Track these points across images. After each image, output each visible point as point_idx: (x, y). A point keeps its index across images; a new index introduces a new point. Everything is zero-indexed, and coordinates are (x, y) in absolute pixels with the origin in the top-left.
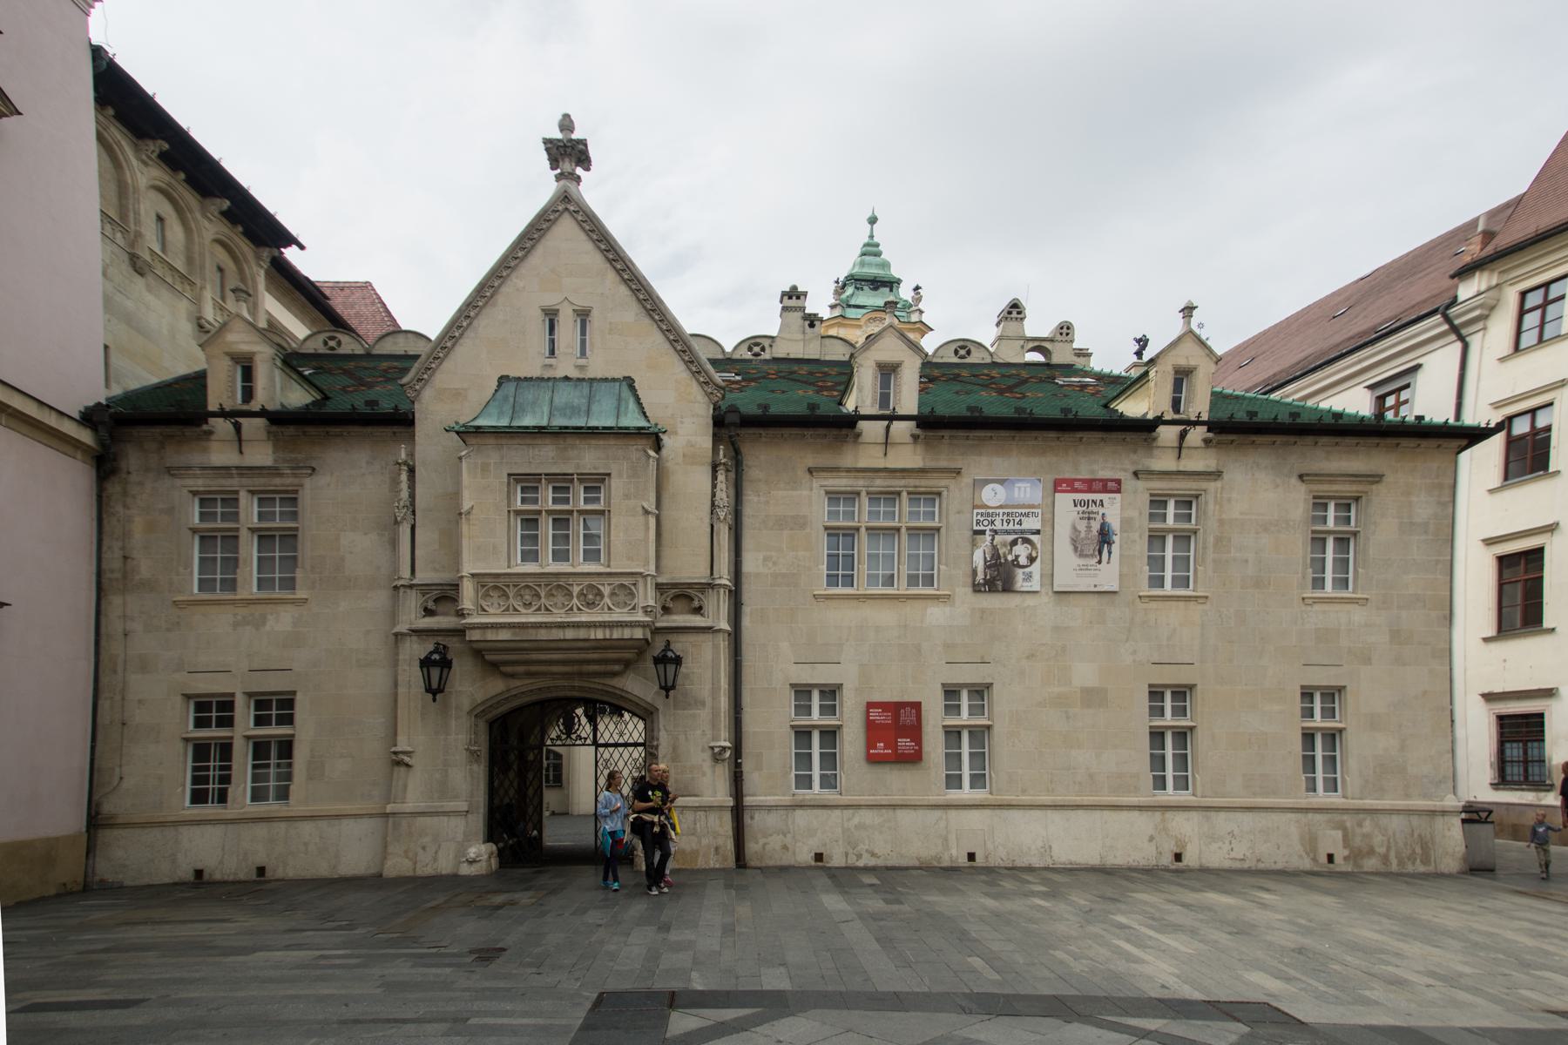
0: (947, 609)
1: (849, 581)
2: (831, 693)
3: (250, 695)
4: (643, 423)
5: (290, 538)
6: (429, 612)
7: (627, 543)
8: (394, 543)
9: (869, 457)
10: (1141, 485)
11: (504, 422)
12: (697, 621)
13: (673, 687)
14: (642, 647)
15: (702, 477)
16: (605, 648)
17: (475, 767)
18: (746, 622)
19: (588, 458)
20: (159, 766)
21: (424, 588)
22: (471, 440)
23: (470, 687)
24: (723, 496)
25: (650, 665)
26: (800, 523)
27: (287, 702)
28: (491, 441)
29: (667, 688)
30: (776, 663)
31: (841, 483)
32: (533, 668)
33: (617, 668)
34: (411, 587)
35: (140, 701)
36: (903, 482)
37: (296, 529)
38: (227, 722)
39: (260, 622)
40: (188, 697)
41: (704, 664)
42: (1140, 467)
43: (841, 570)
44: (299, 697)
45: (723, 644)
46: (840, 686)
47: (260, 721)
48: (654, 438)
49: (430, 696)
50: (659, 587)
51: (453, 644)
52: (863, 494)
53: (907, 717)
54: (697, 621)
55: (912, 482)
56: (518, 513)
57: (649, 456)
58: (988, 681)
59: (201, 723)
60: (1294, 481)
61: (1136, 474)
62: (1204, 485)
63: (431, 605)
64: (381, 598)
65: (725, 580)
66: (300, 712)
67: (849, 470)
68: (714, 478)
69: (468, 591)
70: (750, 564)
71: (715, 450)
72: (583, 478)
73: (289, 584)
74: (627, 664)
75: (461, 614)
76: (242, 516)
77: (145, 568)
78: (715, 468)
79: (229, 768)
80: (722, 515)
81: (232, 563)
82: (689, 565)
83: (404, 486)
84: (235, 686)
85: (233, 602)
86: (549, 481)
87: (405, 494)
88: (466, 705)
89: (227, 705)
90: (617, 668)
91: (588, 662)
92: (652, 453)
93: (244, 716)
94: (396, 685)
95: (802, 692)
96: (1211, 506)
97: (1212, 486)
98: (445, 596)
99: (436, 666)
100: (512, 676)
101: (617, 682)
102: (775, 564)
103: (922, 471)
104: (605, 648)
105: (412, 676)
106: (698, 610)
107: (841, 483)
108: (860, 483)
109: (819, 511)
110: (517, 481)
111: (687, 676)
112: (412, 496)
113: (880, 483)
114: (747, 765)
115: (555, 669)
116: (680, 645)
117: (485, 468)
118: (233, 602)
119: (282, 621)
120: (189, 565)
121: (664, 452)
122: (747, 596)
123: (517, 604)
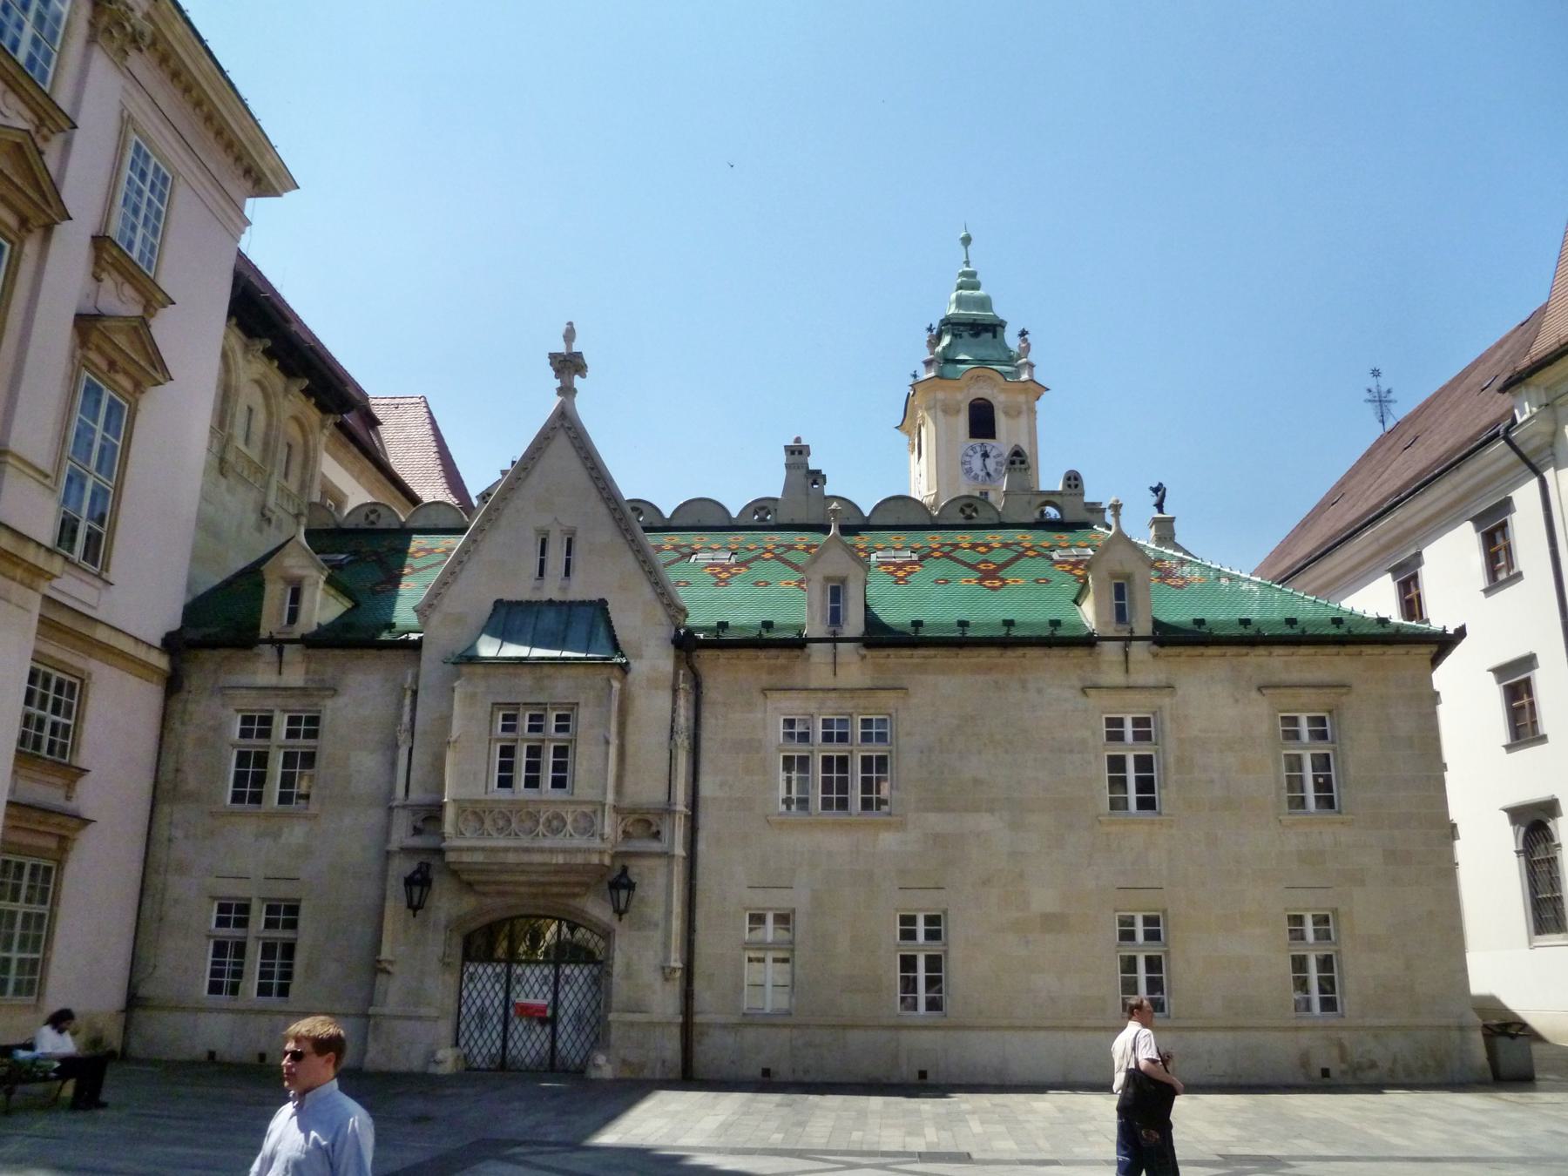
3: (264, 900)
6: (417, 831)
7: (592, 767)
8: (393, 765)
12: (655, 846)
15: (663, 700)
18: (702, 846)
20: (187, 961)
22: (465, 669)
24: (684, 719)
25: (606, 886)
27: (293, 909)
33: (577, 890)
35: (176, 901)
38: (242, 923)
39: (276, 836)
40: (214, 898)
41: (659, 887)
42: (1088, 684)
44: (303, 904)
45: (679, 870)
46: (794, 911)
47: (269, 924)
49: (411, 912)
51: (435, 862)
59: (222, 922)
60: (1254, 694)
61: (1084, 690)
63: (419, 824)
64: (375, 816)
65: (681, 805)
68: (675, 702)
69: (450, 814)
70: (707, 787)
71: (676, 674)
72: (555, 706)
77: (191, 781)
78: (675, 691)
80: (679, 741)
81: (260, 780)
82: (647, 788)
83: (407, 709)
84: (253, 892)
87: (406, 718)
89: (244, 908)
90: (577, 890)
91: (551, 884)
93: (258, 917)
96: (1168, 726)
97: (1166, 701)
98: (431, 815)
99: (418, 883)
100: (484, 894)
101: (577, 903)
105: (396, 888)
106: (657, 835)
111: (642, 900)
112: (413, 720)
114: (699, 985)
116: (637, 869)
119: (295, 834)
120: (225, 779)
121: (630, 677)
122: (703, 820)
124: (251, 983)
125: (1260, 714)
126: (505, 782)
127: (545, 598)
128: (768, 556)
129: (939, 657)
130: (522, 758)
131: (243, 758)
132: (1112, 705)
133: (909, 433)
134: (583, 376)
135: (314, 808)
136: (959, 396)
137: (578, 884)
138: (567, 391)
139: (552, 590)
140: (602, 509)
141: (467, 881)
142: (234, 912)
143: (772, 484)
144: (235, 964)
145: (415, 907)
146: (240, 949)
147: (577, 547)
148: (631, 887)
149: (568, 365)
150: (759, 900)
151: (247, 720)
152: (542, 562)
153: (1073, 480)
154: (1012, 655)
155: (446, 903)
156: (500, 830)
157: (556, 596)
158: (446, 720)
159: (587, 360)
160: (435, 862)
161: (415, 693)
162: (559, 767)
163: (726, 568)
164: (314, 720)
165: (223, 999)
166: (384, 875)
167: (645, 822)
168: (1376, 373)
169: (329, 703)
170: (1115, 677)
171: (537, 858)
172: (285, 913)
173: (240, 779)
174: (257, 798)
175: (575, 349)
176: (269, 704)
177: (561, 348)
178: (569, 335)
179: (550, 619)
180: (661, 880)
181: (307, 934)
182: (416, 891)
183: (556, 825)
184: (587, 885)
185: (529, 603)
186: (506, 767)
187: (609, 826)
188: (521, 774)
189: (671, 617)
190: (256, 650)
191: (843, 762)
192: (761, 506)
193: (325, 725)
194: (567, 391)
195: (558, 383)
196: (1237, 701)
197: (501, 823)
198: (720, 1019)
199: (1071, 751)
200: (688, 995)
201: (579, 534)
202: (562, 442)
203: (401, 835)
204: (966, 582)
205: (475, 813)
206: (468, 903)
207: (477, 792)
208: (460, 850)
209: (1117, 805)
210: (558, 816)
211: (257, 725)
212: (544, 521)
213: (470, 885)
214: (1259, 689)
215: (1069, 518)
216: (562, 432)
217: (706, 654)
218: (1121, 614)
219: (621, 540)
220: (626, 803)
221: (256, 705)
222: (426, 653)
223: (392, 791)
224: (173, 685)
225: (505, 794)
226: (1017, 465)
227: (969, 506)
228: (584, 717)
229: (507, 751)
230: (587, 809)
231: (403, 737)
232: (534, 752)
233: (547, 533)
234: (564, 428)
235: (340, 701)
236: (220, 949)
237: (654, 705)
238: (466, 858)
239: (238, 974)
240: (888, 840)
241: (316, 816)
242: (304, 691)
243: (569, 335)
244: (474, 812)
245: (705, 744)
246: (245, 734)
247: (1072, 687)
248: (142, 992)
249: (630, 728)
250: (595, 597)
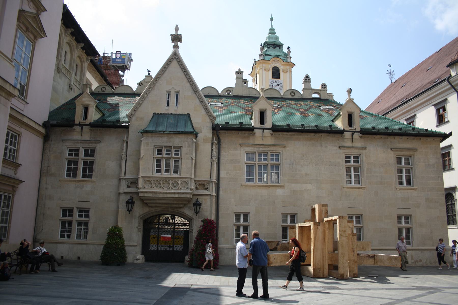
0: (283, 190)
1: (253, 180)
3: (77, 208)
4: (192, 130)
5: (92, 163)
6: (129, 187)
8: (120, 165)
9: (258, 141)
10: (341, 151)
11: (154, 129)
12: (206, 192)
13: (199, 213)
14: (189, 200)
15: (209, 146)
16: (178, 200)
17: (139, 233)
18: (221, 192)
19: (177, 141)
20: (53, 228)
21: (128, 180)
22: (145, 135)
23: (139, 210)
24: (215, 153)
25: (192, 205)
27: (87, 211)
28: (150, 135)
29: (197, 213)
31: (250, 149)
32: (157, 205)
33: (181, 206)
34: (124, 179)
35: (49, 208)
36: (268, 149)
37: (94, 159)
38: (71, 216)
40: (61, 208)
45: (214, 199)
47: (80, 216)
48: (196, 136)
49: (128, 212)
50: (195, 181)
51: (135, 196)
52: (257, 152)
54: (206, 192)
55: (271, 149)
56: (156, 158)
57: (193, 141)
58: (296, 212)
59: (64, 215)
60: (389, 150)
61: (339, 148)
62: (361, 151)
63: (129, 184)
64: (115, 182)
65: (214, 179)
66: (91, 214)
67: (252, 145)
68: (212, 147)
71: (213, 138)
72: (174, 147)
73: (90, 176)
74: (185, 205)
75: (137, 187)
76: (80, 155)
78: (212, 144)
79: (71, 229)
80: (214, 159)
81: (76, 170)
83: (125, 148)
84: (74, 205)
85: (75, 181)
86: (165, 148)
87: (125, 150)
88: (138, 215)
89: (71, 211)
90: (181, 206)
91: (173, 204)
92: (194, 140)
93: (76, 214)
94: (118, 208)
96: (364, 159)
97: (364, 152)
99: (130, 203)
100: (151, 207)
101: (182, 210)
102: (230, 175)
103: (274, 146)
104: (178, 200)
106: (207, 189)
107: (250, 149)
108: (256, 149)
109: (243, 158)
110: (156, 148)
112: (127, 151)
113: (262, 149)
115: (163, 205)
116: (201, 199)
117: (148, 144)
118: (75, 181)
119: (88, 187)
120: (64, 169)
121: (198, 138)
122: (221, 185)
123: (153, 185)
124: (74, 234)
125: (391, 157)
126: (158, 171)
127: (170, 113)
128: (233, 104)
129: (296, 135)
130: (163, 164)
131: (69, 163)
132: (348, 151)
133: (252, 76)
134: (181, 42)
135: (94, 179)
136: (270, 66)
137: (182, 204)
138: (176, 47)
139: (172, 110)
140: (188, 85)
141: (145, 202)
142: (68, 212)
143: (232, 83)
144: (68, 228)
145: (129, 211)
146: (70, 223)
147: (180, 96)
149: (176, 39)
150: (239, 210)
151: (70, 150)
152: (168, 101)
153: (324, 86)
154: (318, 135)
155: (139, 210)
156: (157, 186)
157: (174, 112)
158: (138, 151)
159: (183, 37)
160: (135, 196)
161: (127, 142)
162: (176, 166)
164: (93, 151)
165: (66, 240)
166: (118, 201)
167: (202, 185)
168: (390, 66)
169: (98, 145)
170: (349, 144)
171: (169, 196)
172: (84, 212)
173: (69, 170)
174: (75, 176)
175: (179, 33)
176: (78, 145)
177: (174, 33)
178: (177, 29)
179: (172, 120)
180: (208, 203)
181: (92, 218)
182: (130, 205)
183: (175, 184)
184: (185, 205)
185: (164, 114)
186: (159, 166)
187: (193, 186)
188: (163, 169)
189: (211, 120)
190: (74, 128)
192: (228, 90)
193: (97, 153)
194: (176, 47)
195: (173, 44)
196: (384, 152)
197: (157, 184)
198: (226, 246)
199: (335, 166)
201: (181, 92)
202: (175, 63)
203: (124, 188)
204: (297, 114)
205: (148, 181)
206: (146, 210)
208: (144, 192)
210: (175, 182)
211: (74, 152)
212: (169, 88)
213: (147, 204)
214: (391, 149)
215: (322, 98)
216: (175, 59)
217: (222, 132)
218: (350, 125)
219: (195, 95)
220: (197, 179)
221: (73, 145)
222: (131, 129)
223: (120, 174)
224: (46, 138)
225: (158, 175)
226: (307, 81)
227: (293, 92)
228: (184, 150)
229: (159, 161)
230: (186, 180)
231: (124, 156)
232: (168, 160)
233: (170, 92)
234: (175, 58)
235: (102, 145)
236: (64, 223)
237: (206, 148)
238: (146, 195)
239: (70, 232)
240: (279, 192)
241: (94, 181)
242: (89, 141)
243: (177, 29)
244: (148, 180)
245: (222, 161)
246: (70, 155)
247: (336, 146)
248: (38, 237)
249: (198, 155)
250: (186, 113)
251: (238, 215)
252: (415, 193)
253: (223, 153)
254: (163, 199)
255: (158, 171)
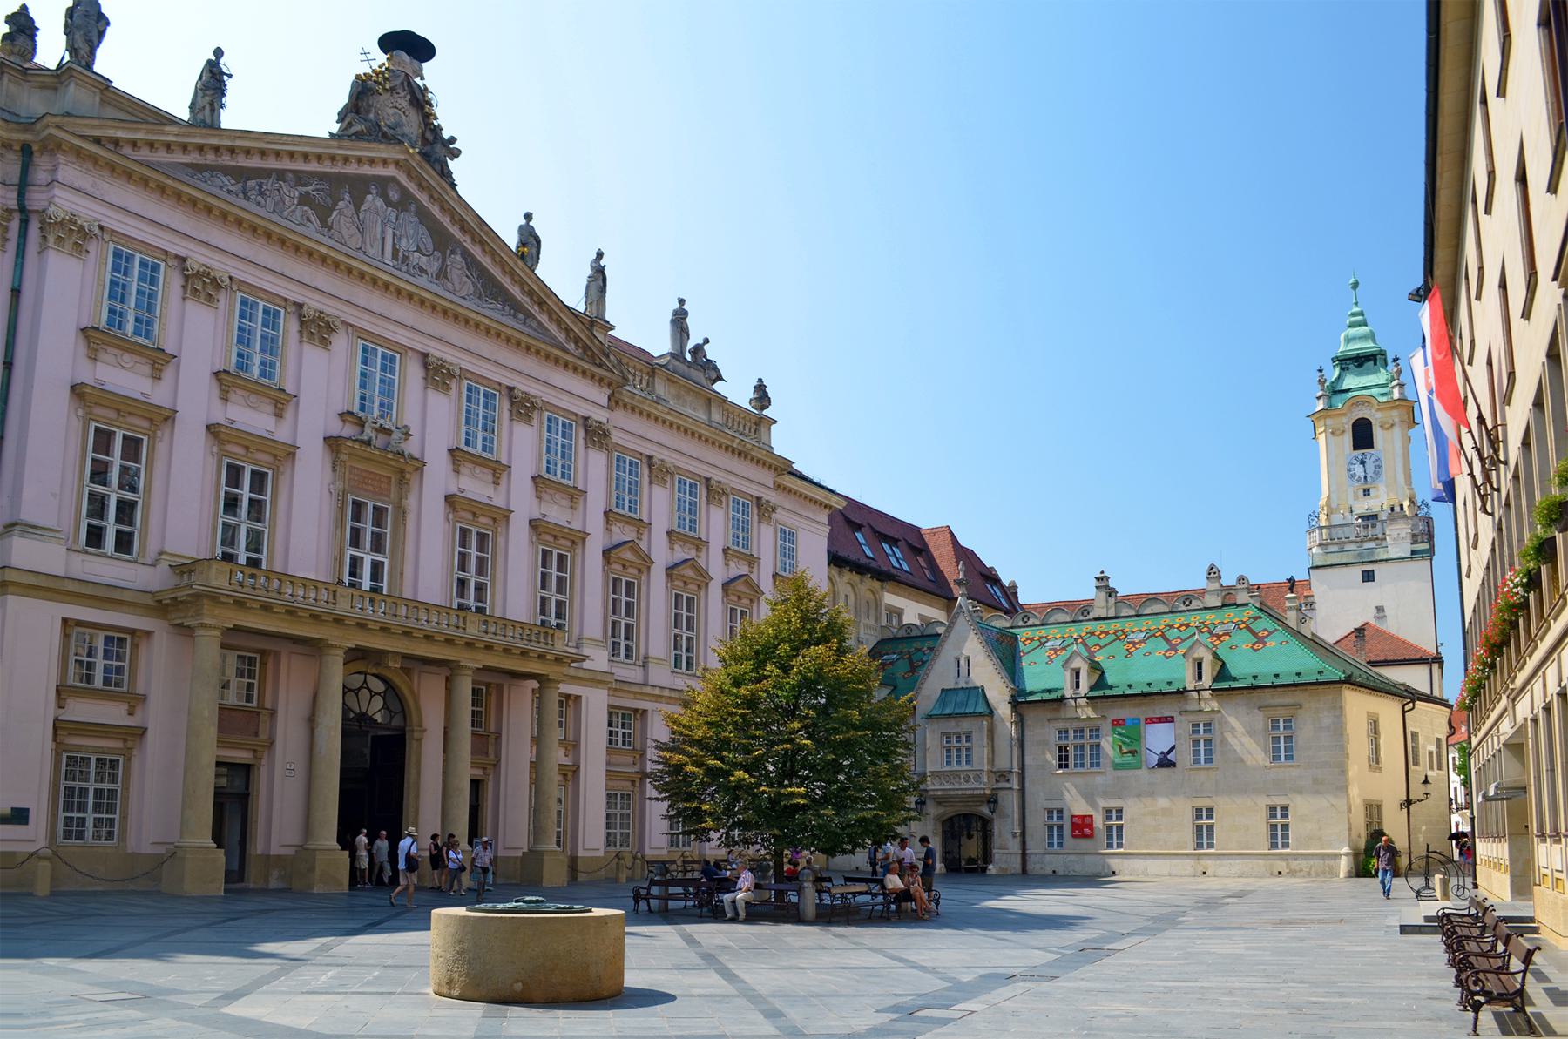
2: (1060, 811)
26: (1045, 743)
30: (1038, 800)
31: (1061, 725)
41: (1010, 802)
43: (1063, 761)
53: (1087, 821)
65: (1016, 769)
82: (1003, 763)
95: (1050, 812)
107: (1061, 725)
113: (1076, 724)
126: (949, 763)
130: (954, 754)
141: (940, 801)
148: (996, 802)
150: (1050, 806)
163: (1056, 651)
167: (1003, 775)
191: (1082, 746)
200: (1024, 844)
207: (938, 768)
209: (1196, 761)
228: (975, 736)
240: (1099, 779)
251: (1050, 812)
252: (1295, 772)
253: (1028, 734)
254: (957, 796)
255: (949, 763)
